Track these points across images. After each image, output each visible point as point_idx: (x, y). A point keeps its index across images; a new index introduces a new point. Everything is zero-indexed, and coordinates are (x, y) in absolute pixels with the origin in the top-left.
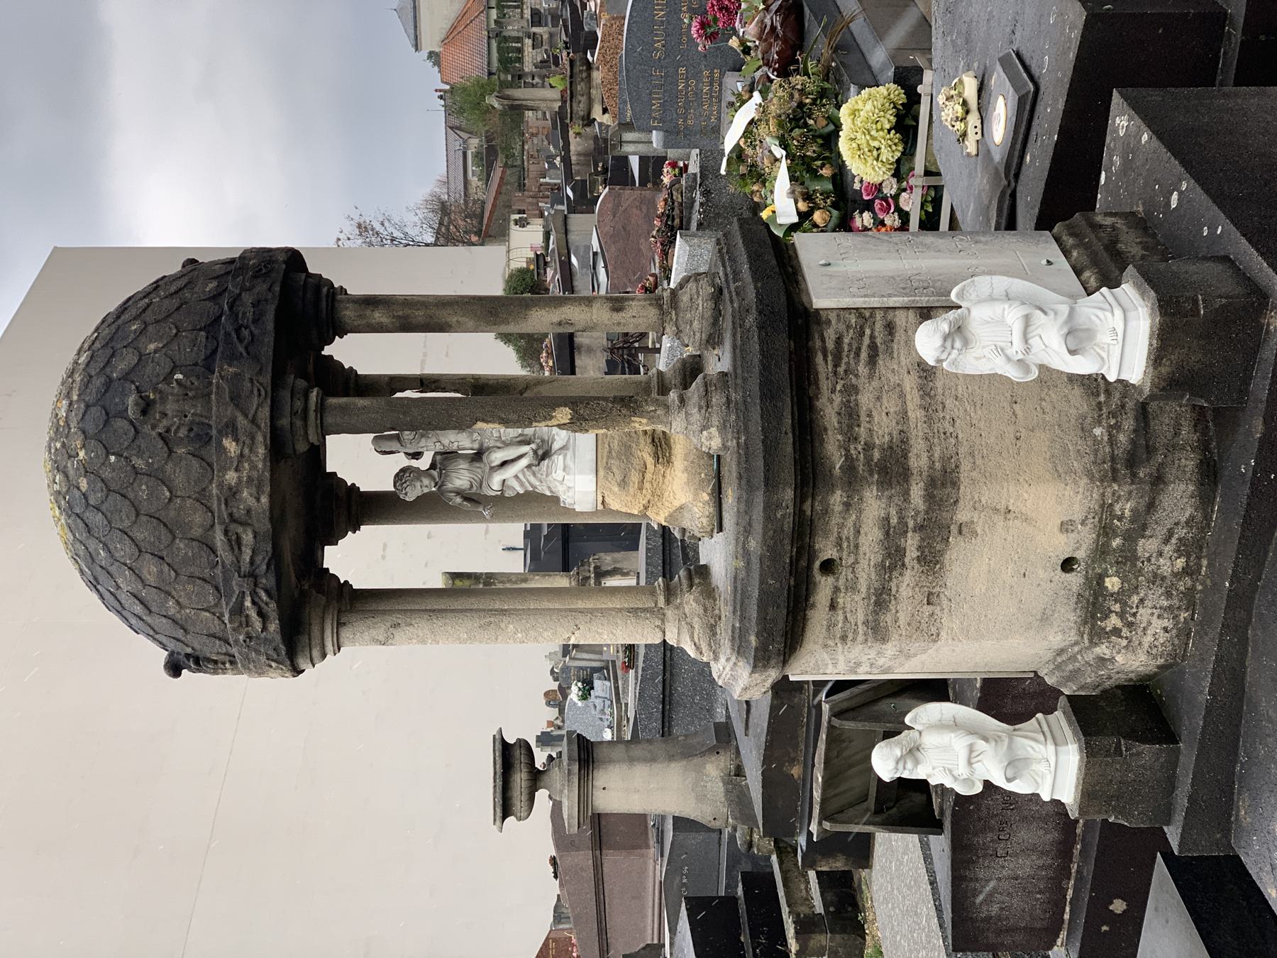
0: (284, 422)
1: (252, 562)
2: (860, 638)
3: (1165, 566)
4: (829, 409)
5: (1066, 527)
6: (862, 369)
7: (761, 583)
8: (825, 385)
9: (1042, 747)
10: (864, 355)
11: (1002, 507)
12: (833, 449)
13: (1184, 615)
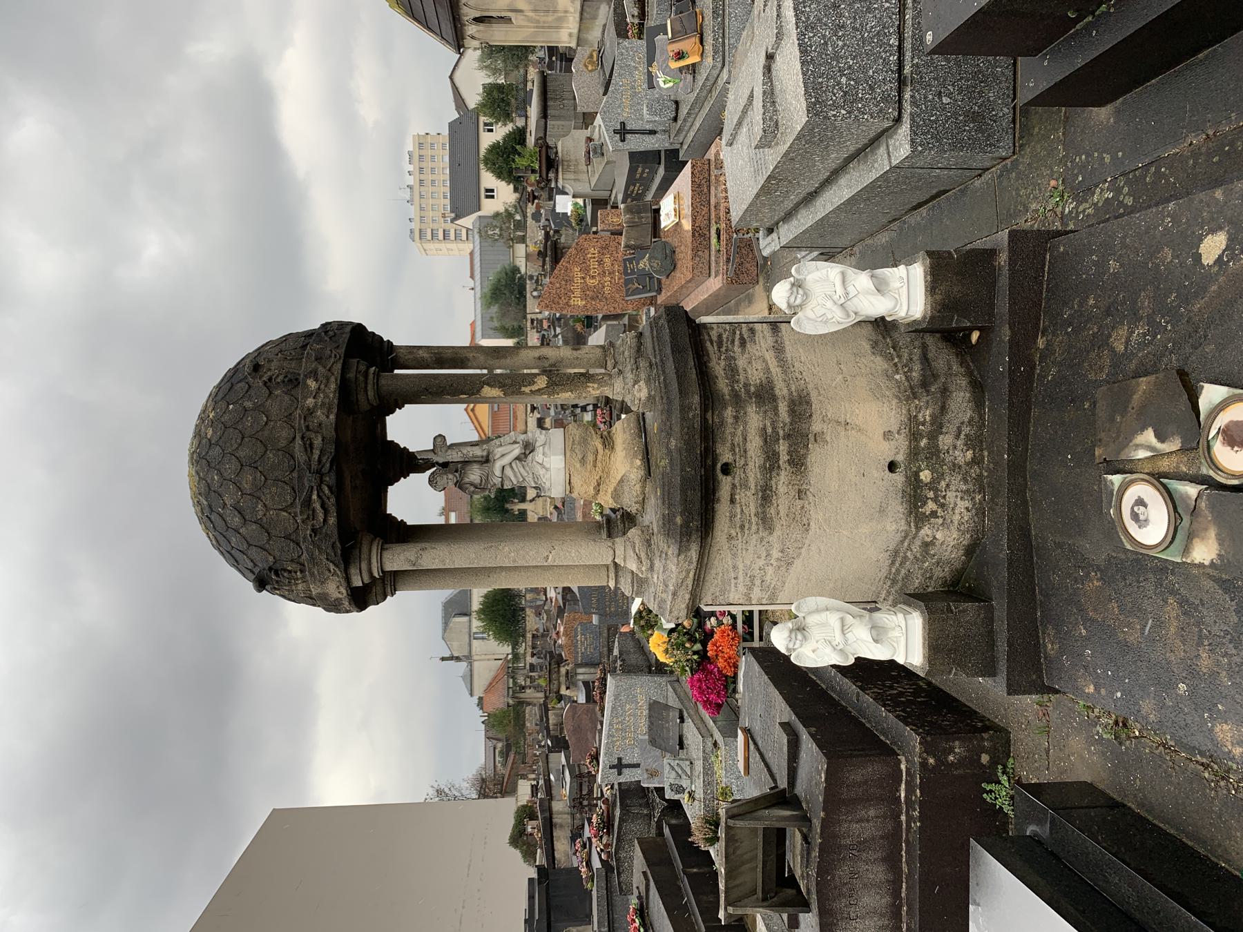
0: (351, 375)
1: (320, 461)
2: (754, 528)
3: (961, 460)
4: (718, 367)
5: (887, 435)
6: (737, 349)
7: (682, 470)
8: (714, 357)
10: (737, 343)
11: (842, 420)
12: (723, 385)
13: (978, 497)
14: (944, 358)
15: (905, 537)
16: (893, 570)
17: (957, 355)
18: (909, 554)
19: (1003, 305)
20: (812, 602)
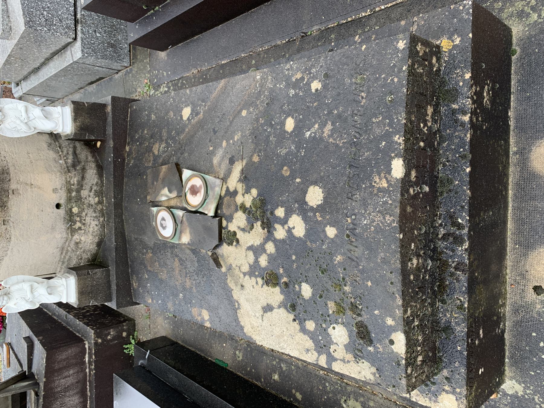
5: (55, 190)
9: (60, 281)
11: (29, 182)
13: (102, 219)
14: (84, 154)
15: (67, 240)
16: (62, 257)
17: (91, 152)
18: (69, 248)
19: (110, 130)
20: (14, 278)
